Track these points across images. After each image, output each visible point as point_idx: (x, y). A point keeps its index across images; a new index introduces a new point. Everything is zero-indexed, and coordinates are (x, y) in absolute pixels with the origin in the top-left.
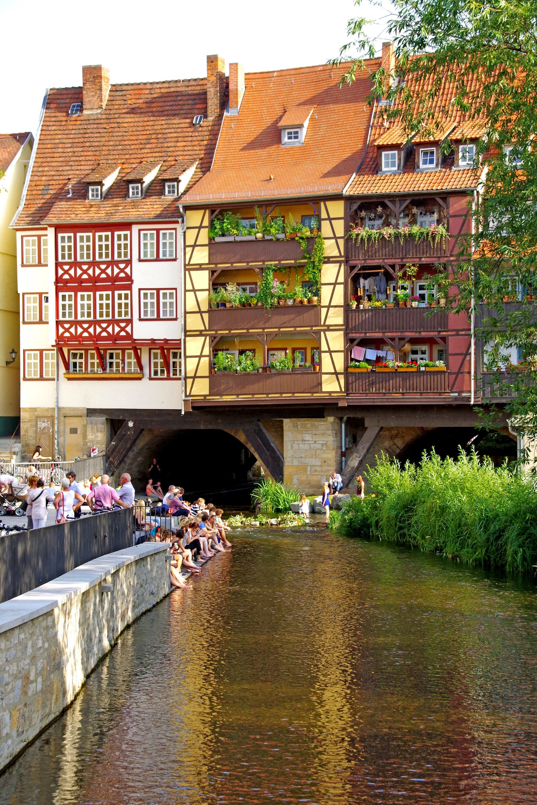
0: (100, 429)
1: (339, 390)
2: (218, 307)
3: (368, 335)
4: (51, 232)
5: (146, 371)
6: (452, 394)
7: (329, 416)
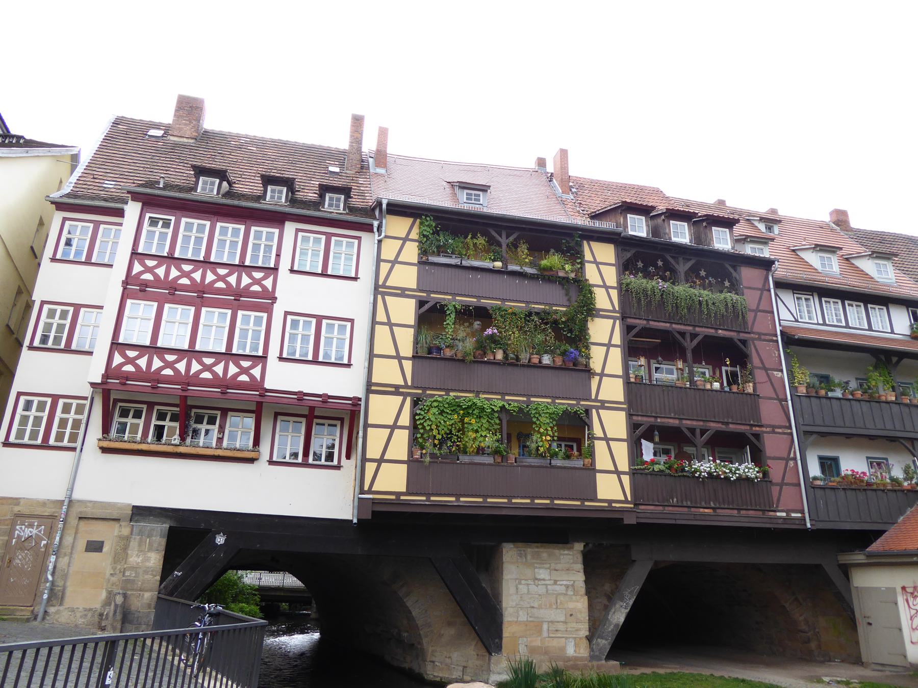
0: (155, 545)
1: (623, 499)
2: (430, 352)
3: (659, 420)
4: (133, 209)
5: (265, 448)
6: (779, 514)
7: (578, 542)
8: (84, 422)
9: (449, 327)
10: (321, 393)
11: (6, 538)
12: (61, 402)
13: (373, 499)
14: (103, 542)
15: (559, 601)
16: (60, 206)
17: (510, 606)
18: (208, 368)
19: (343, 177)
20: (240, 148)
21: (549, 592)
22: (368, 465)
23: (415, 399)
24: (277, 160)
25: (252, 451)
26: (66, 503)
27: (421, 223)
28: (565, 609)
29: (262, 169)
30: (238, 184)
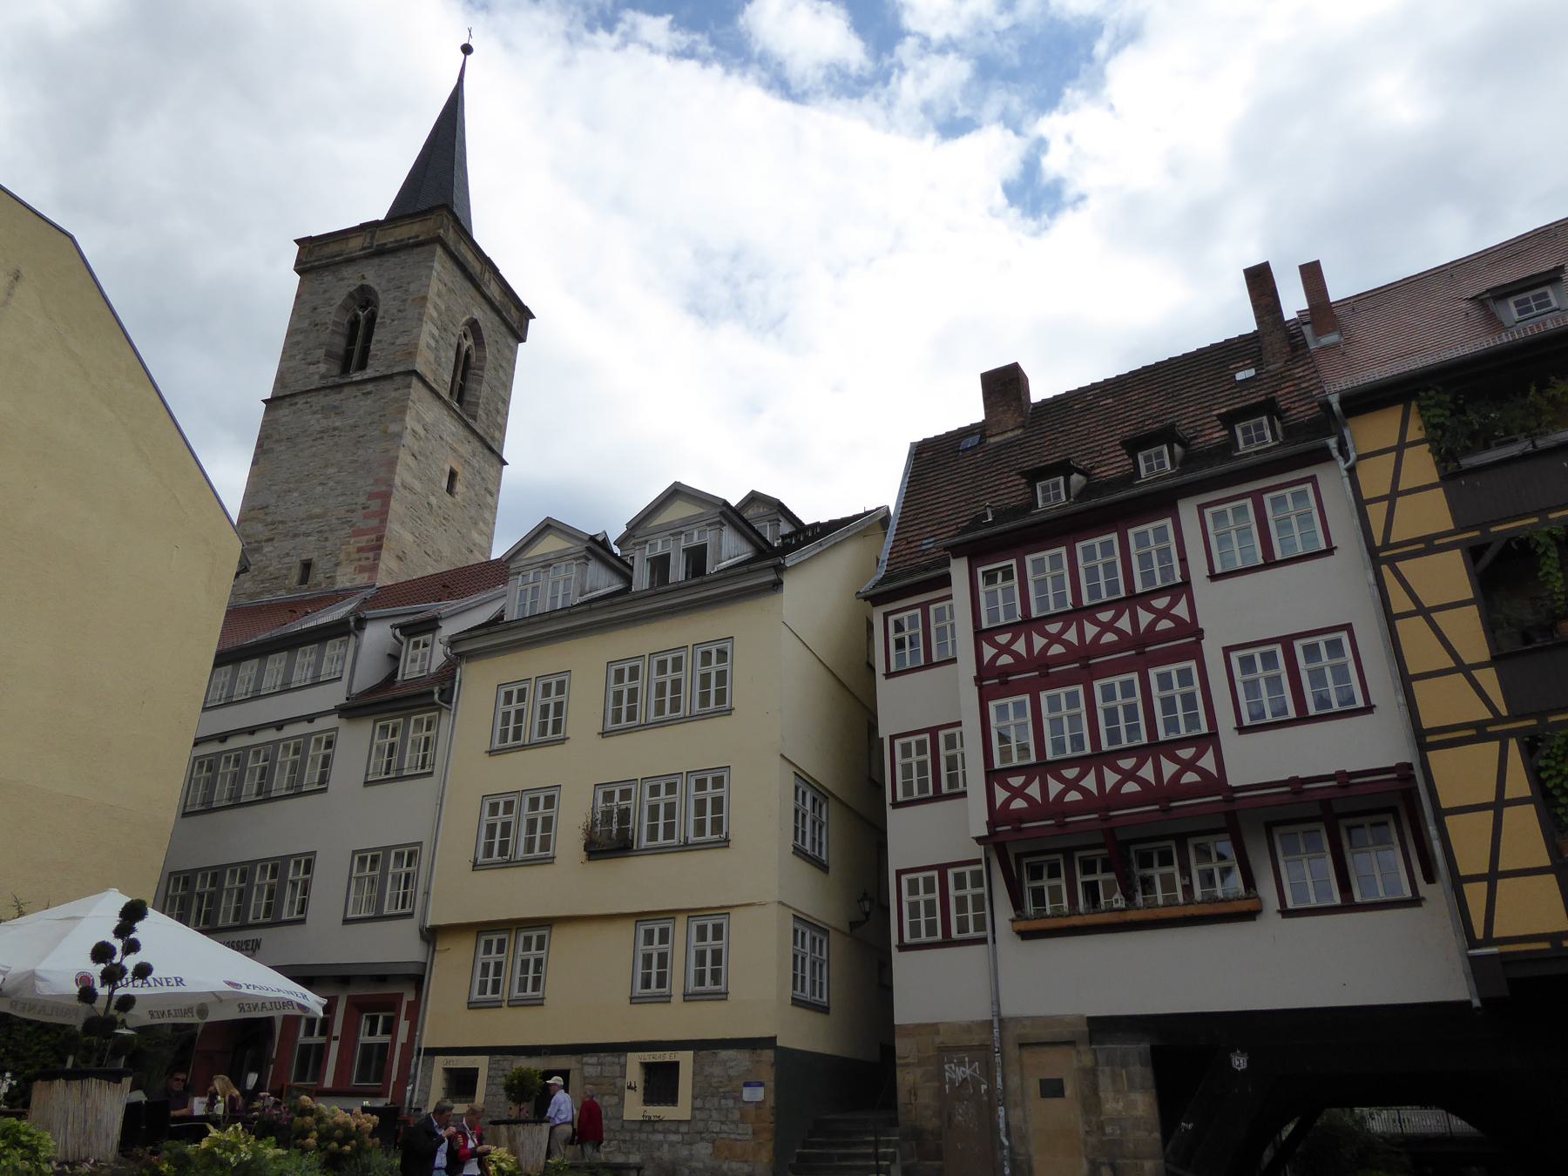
2: (1527, 639)
4: (959, 570)
5: (1267, 890)
8: (986, 897)
9: (1552, 578)
10: (1333, 772)
11: (936, 1084)
12: (951, 873)
13: (1501, 955)
14: (1060, 1081)
16: (875, 599)
18: (1130, 775)
19: (1265, 381)
20: (1088, 410)
22: (1467, 888)
23: (1528, 739)
24: (1148, 403)
25: (1246, 899)
26: (996, 1024)
27: (1420, 408)
29: (1127, 429)
30: (1098, 467)
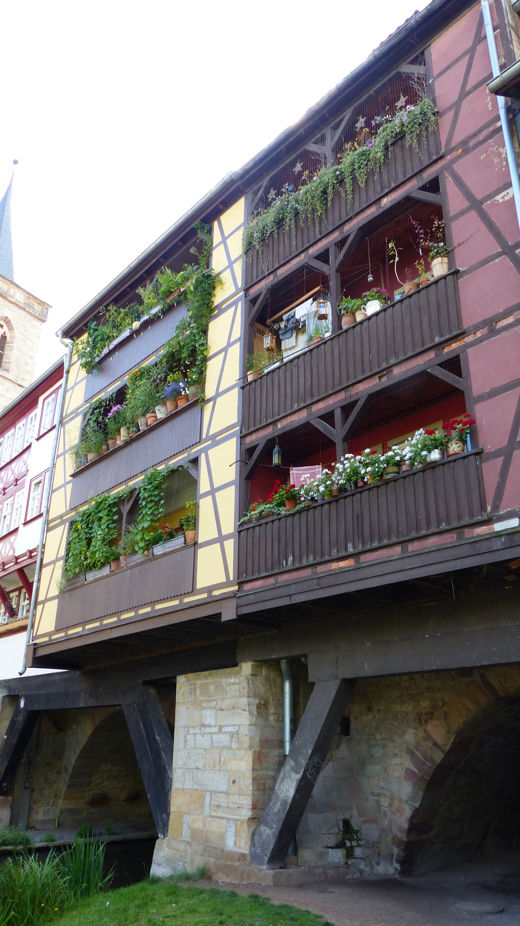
15: (222, 759)
17: (179, 766)
21: (213, 745)
28: (228, 771)
